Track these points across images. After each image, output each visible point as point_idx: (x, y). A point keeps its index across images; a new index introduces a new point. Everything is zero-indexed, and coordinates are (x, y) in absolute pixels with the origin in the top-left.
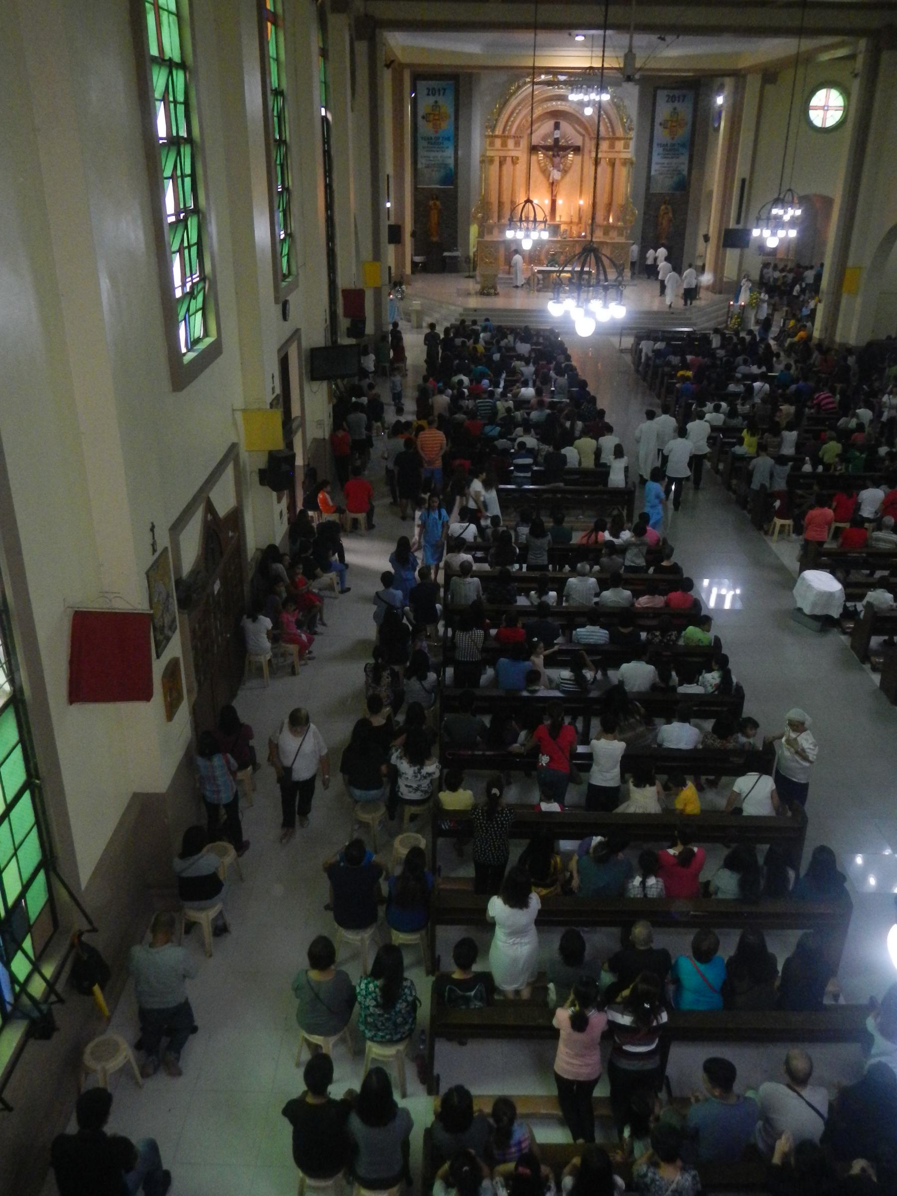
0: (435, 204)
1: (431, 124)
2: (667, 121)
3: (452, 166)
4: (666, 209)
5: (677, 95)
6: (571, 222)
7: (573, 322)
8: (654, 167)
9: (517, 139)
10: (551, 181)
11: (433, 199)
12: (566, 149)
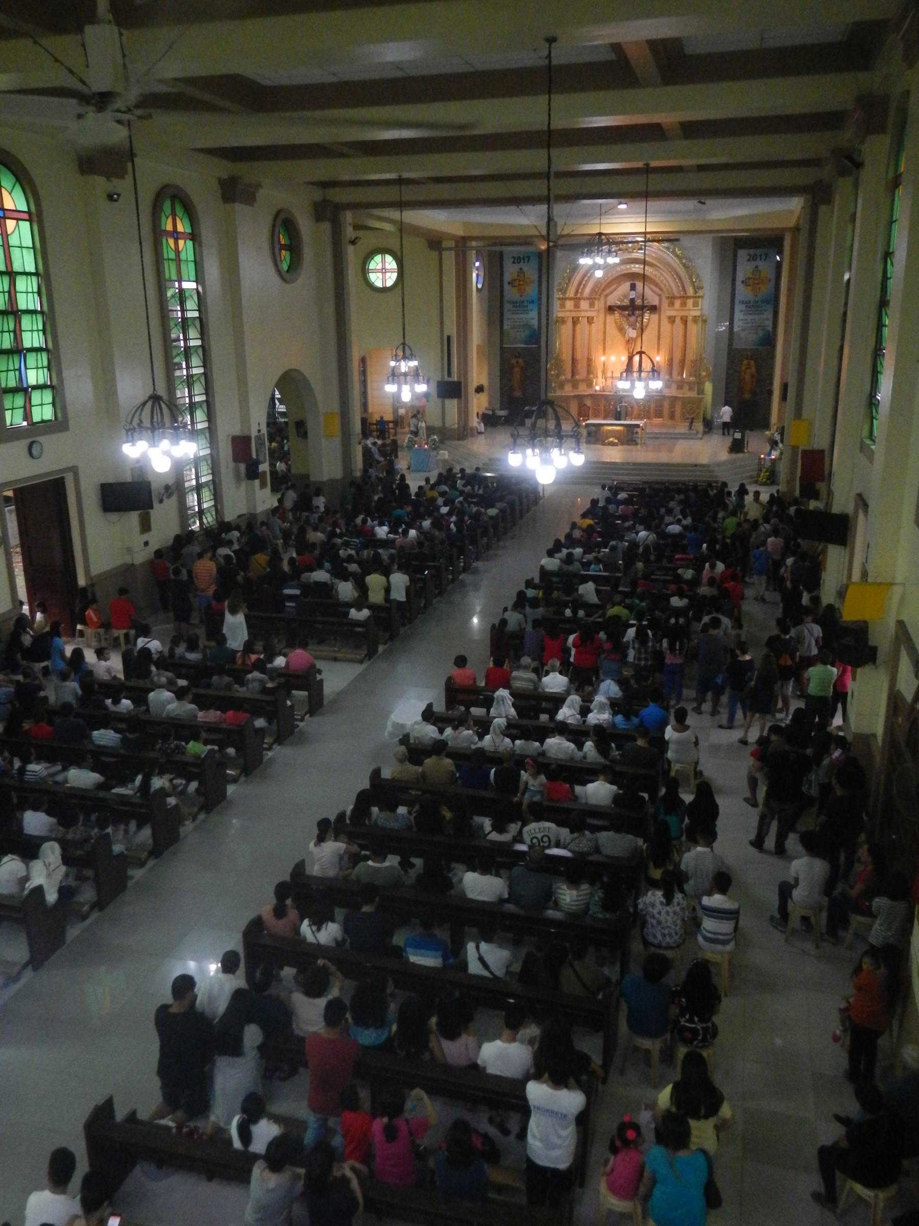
0: (517, 362)
1: (515, 290)
2: (749, 279)
3: (536, 327)
4: (749, 364)
7: (150, 459)
9: (592, 300)
11: (516, 357)
12: (642, 308)
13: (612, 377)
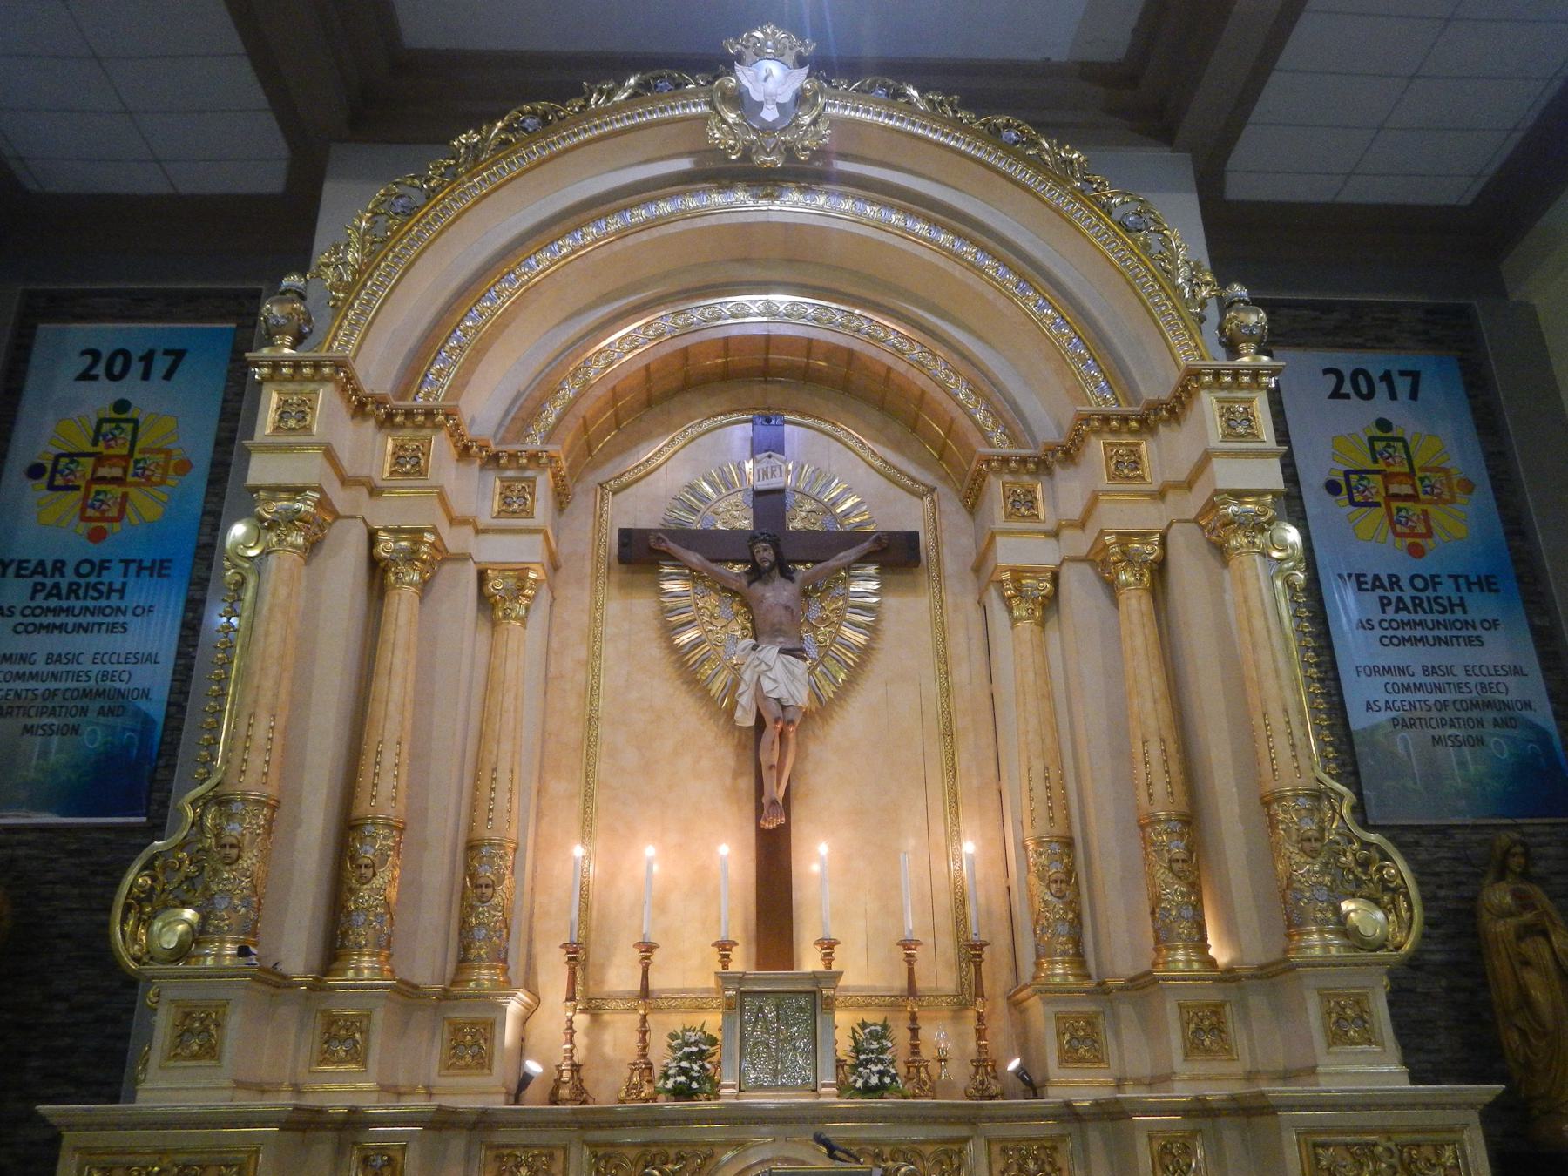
3: (156, 708)
4: (1523, 901)
5: (1376, 374)
6: (912, 990)
8: (1359, 692)
10: (746, 719)
13: (645, 993)
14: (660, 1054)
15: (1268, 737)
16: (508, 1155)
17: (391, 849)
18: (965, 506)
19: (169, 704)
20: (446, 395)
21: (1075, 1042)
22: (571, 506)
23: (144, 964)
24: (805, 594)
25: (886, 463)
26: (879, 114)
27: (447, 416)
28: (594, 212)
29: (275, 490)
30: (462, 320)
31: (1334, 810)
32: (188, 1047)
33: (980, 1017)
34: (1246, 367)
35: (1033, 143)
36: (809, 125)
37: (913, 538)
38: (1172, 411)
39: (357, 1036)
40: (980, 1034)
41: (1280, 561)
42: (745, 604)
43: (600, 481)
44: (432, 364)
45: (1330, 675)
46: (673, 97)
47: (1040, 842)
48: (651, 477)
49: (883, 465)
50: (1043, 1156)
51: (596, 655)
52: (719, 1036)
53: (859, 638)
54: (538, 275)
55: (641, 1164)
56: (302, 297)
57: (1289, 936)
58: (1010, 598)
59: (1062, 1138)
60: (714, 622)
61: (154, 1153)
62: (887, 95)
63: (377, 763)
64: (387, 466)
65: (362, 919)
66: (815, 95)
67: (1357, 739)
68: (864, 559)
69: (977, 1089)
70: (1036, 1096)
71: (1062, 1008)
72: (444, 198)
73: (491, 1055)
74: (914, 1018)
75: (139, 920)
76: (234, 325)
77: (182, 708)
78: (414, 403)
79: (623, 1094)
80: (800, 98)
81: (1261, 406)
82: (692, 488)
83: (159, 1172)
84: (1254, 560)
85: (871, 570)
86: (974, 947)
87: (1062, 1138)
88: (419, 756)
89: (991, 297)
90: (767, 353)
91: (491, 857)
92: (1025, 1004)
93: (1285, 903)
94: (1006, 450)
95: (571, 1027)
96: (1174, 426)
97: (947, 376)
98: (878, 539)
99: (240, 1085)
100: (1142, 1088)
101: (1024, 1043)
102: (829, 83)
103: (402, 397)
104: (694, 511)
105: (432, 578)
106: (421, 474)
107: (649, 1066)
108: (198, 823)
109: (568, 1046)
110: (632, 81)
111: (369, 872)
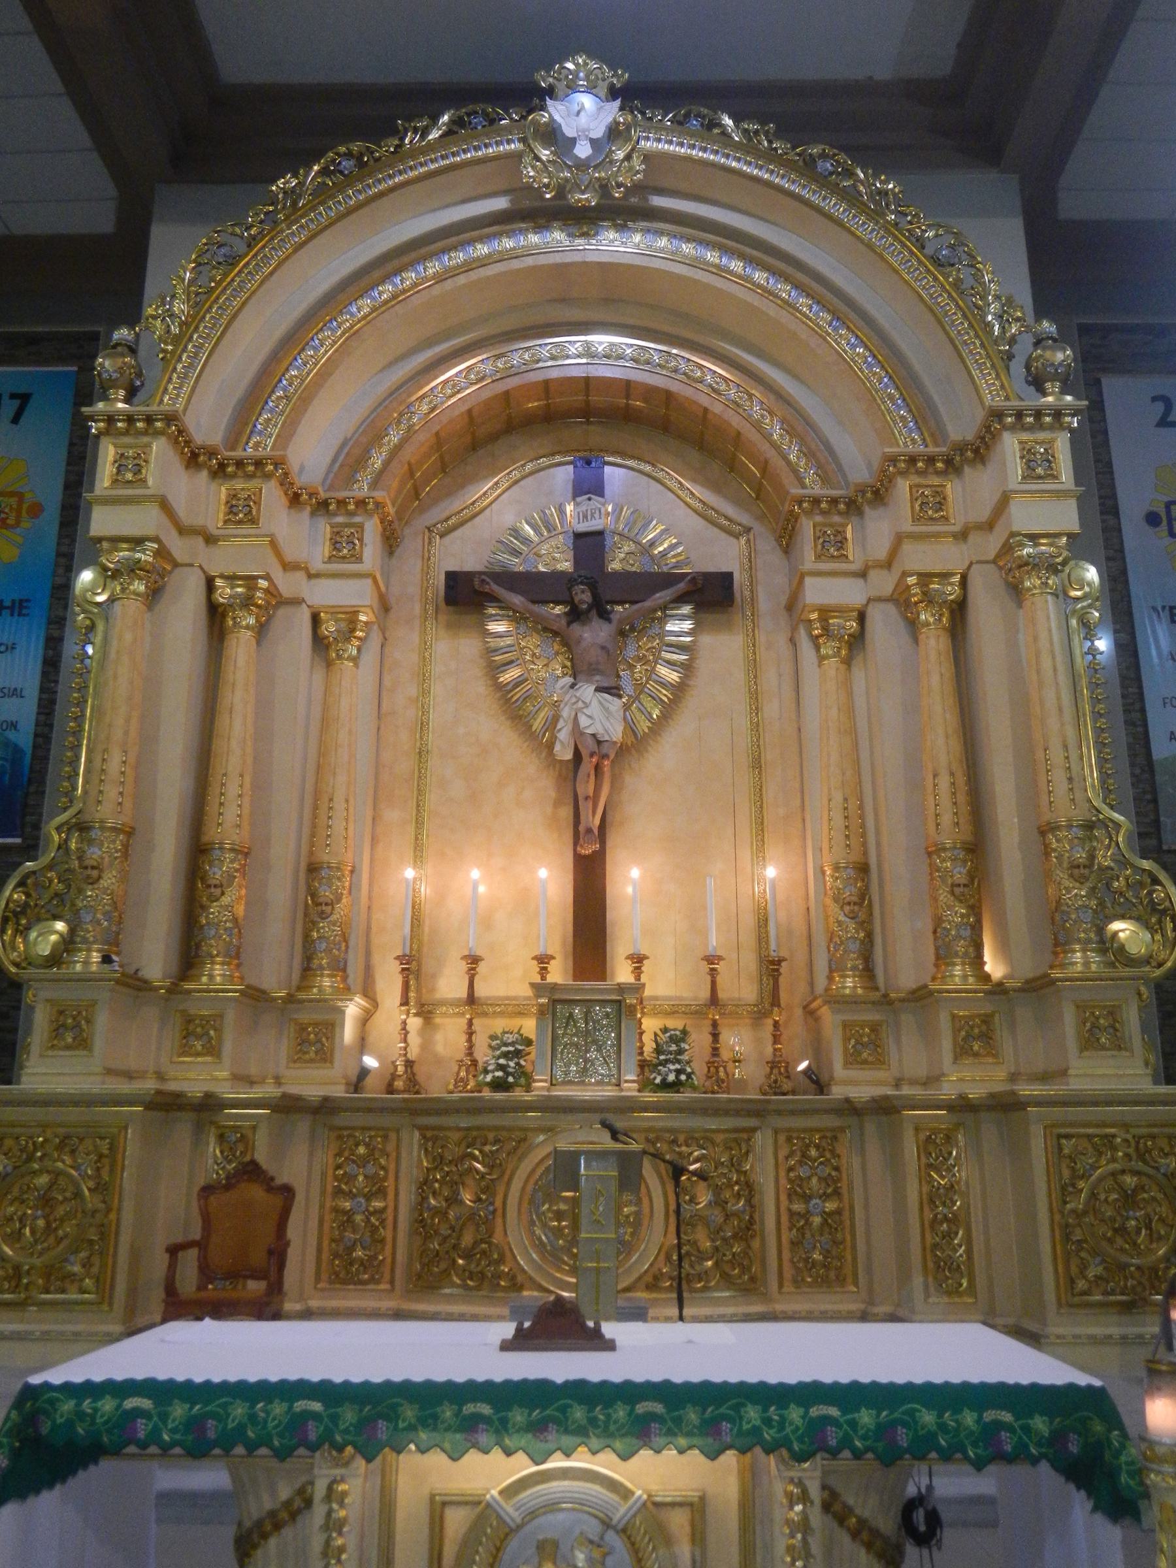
3: (24, 738)
6: (714, 1000)
13: (471, 999)
14: (483, 1054)
15: (1048, 771)
16: (349, 1136)
17: (237, 870)
18: (780, 545)
19: (36, 735)
20: (274, 445)
21: (859, 1047)
22: (399, 550)
23: (24, 968)
24: (622, 633)
25: (704, 503)
26: (693, 147)
27: (276, 465)
28: (413, 255)
29: (116, 540)
30: (287, 370)
31: (1111, 839)
32: (64, 1039)
33: (776, 1024)
34: (1049, 406)
35: (849, 173)
36: (623, 161)
37: (728, 577)
38: (976, 451)
39: (212, 1033)
40: (776, 1039)
41: (1077, 599)
42: (565, 643)
43: (428, 524)
44: (260, 414)
45: (1137, 706)
46: (487, 135)
47: (836, 868)
48: (477, 519)
49: (701, 505)
50: (824, 1144)
51: (425, 693)
52: (533, 1037)
53: (673, 676)
54: (359, 321)
55: (464, 1145)
56: (133, 351)
57: (1056, 954)
58: (817, 637)
59: (842, 1129)
60: (536, 661)
61: (38, 1126)
62: (702, 125)
63: (222, 794)
64: (221, 516)
65: (213, 932)
66: (628, 128)
67: (1157, 768)
68: (680, 600)
69: (770, 1086)
70: (821, 1092)
71: (848, 1017)
72: (264, 247)
73: (332, 1055)
74: (715, 1024)
75: (17, 931)
76: (75, 369)
77: (47, 739)
78: (244, 454)
79: (451, 1087)
80: (614, 133)
81: (1062, 445)
82: (516, 532)
83: (43, 1142)
84: (1047, 601)
85: (686, 609)
86: (772, 962)
87: (842, 1129)
88: (261, 786)
89: (804, 336)
90: (588, 396)
91: (330, 879)
92: (819, 1013)
93: (1053, 923)
94: (818, 490)
95: (404, 1029)
96: (980, 466)
97: (762, 416)
98: (694, 579)
99: (109, 1072)
100: (919, 1087)
101: (818, 1050)
102: (643, 114)
103: (233, 449)
104: (516, 553)
105: (268, 621)
106: (253, 523)
107: (475, 1063)
108: (63, 846)
109: (402, 1045)
110: (446, 118)
111: (218, 891)
